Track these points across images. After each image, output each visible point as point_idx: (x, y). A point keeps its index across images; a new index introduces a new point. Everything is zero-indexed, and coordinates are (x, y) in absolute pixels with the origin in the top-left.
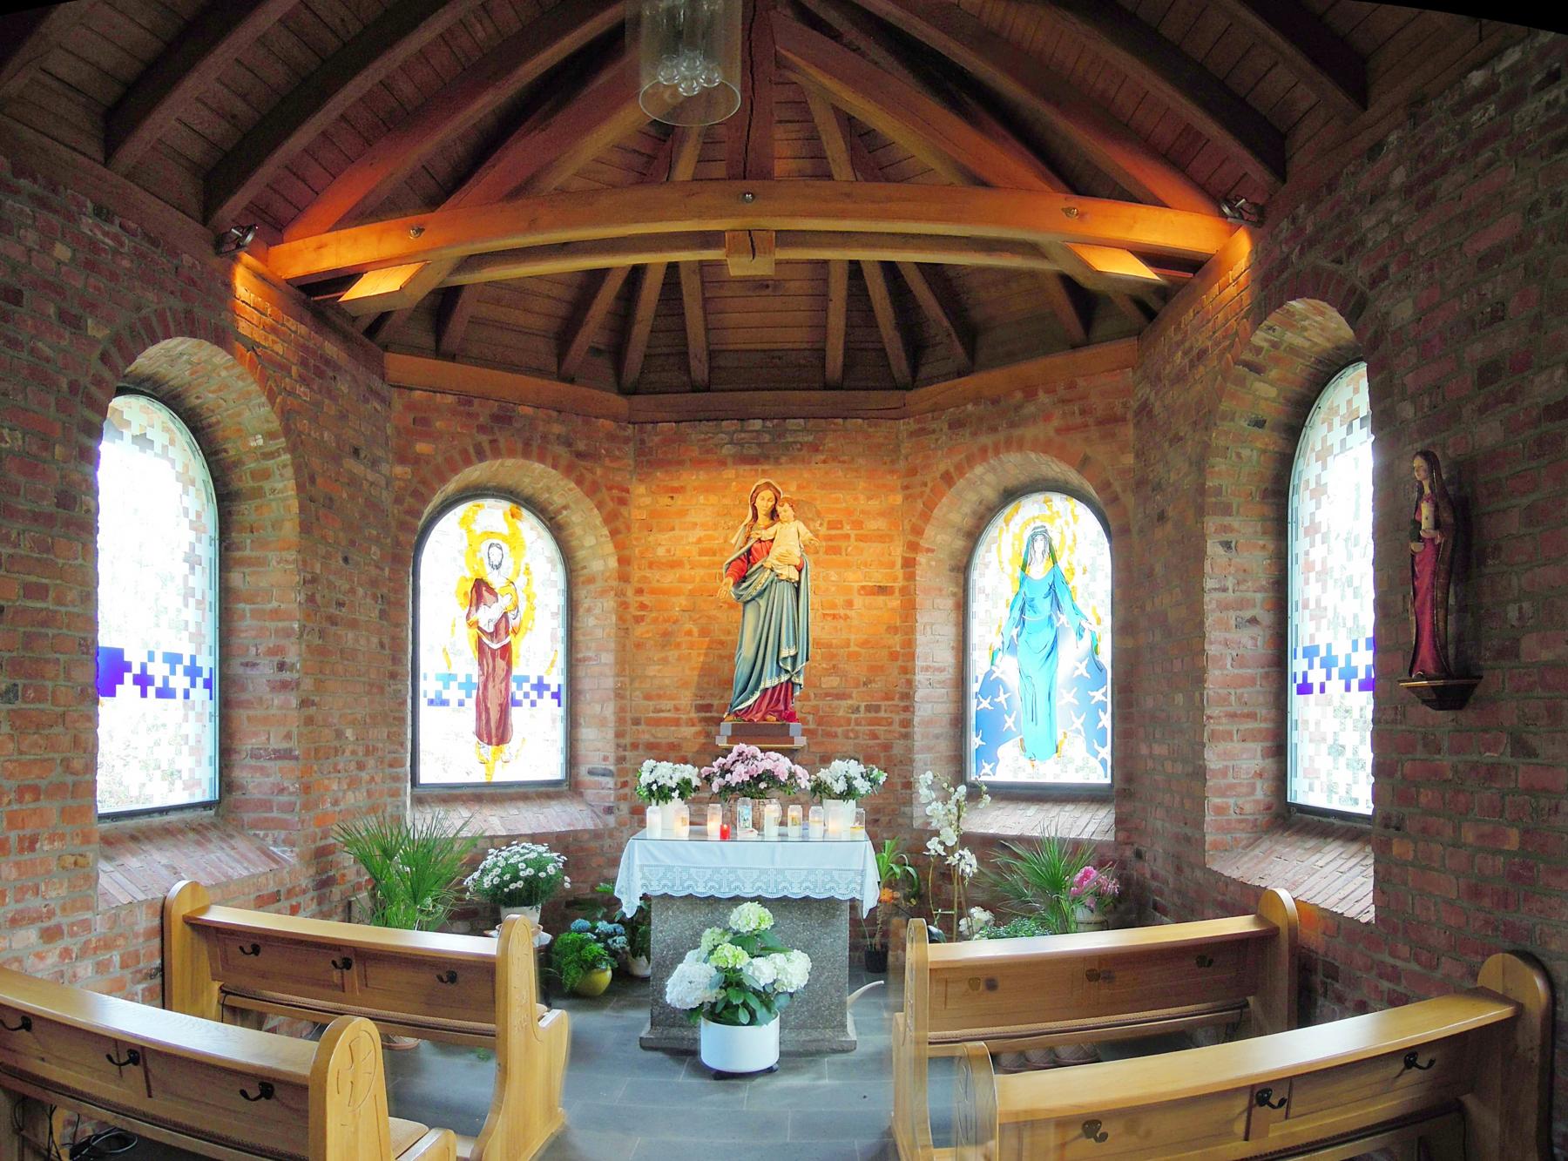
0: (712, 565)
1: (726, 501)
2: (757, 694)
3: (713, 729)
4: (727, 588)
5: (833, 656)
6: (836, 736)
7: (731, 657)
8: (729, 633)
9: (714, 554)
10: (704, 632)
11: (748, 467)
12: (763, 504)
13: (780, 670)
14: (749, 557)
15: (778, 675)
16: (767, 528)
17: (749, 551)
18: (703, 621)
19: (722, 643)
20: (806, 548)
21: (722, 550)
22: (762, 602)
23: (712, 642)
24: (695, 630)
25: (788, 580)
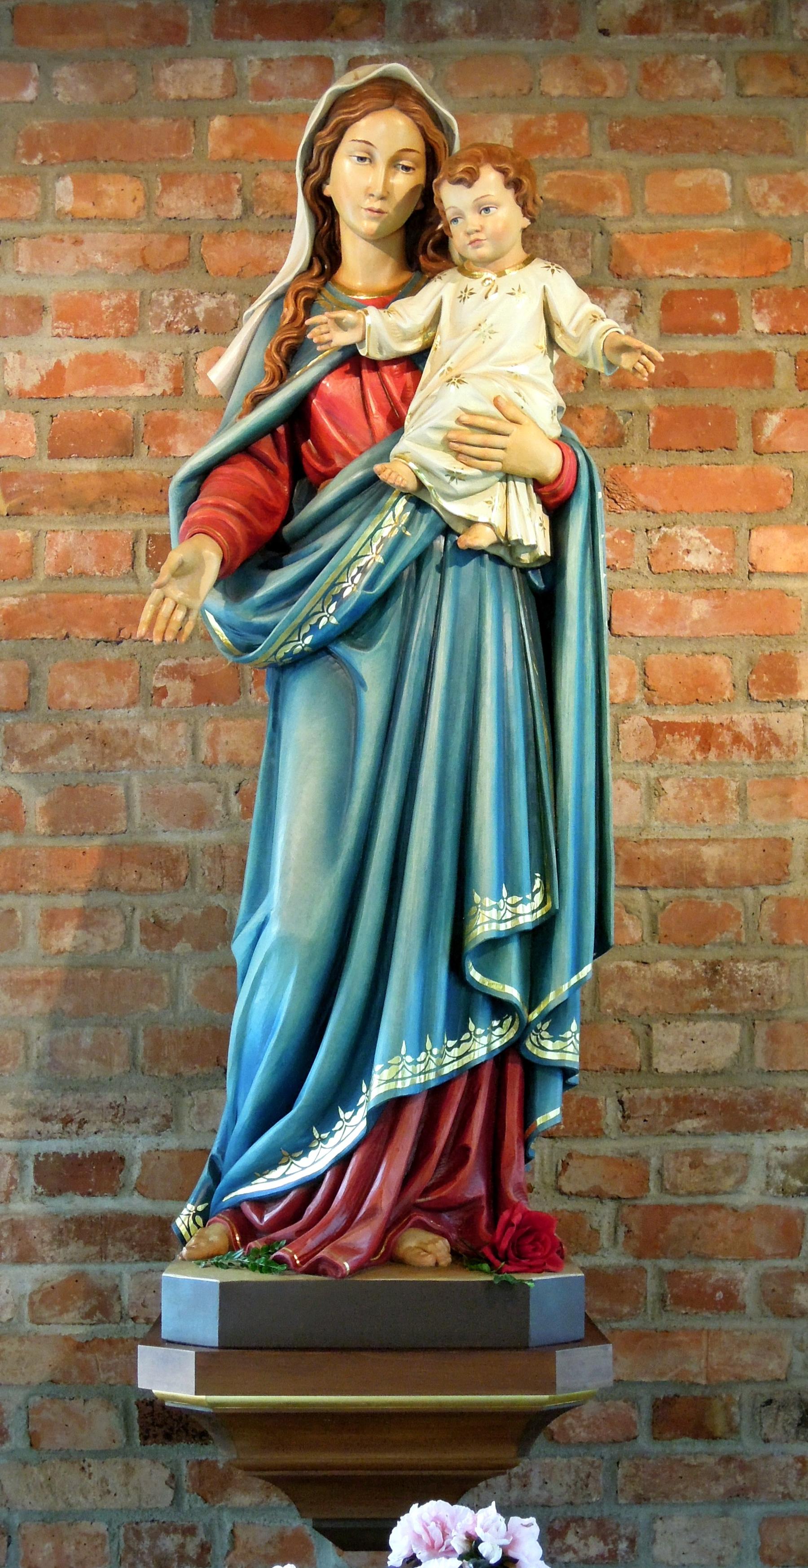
0: (115, 496)
1: (185, 203)
2: (351, 1127)
3: (124, 1273)
4: (188, 588)
5: (698, 927)
6: (730, 1302)
7: (217, 929)
8: (200, 818)
9: (126, 447)
10: (75, 809)
11: (281, 49)
12: (368, 179)
13: (466, 1004)
14: (293, 443)
15: (457, 1029)
16: (384, 302)
17: (298, 418)
18: (75, 756)
19: (169, 865)
20: (579, 386)
21: (163, 428)
22: (370, 664)
23: (116, 855)
24: (35, 804)
25: (504, 554)
